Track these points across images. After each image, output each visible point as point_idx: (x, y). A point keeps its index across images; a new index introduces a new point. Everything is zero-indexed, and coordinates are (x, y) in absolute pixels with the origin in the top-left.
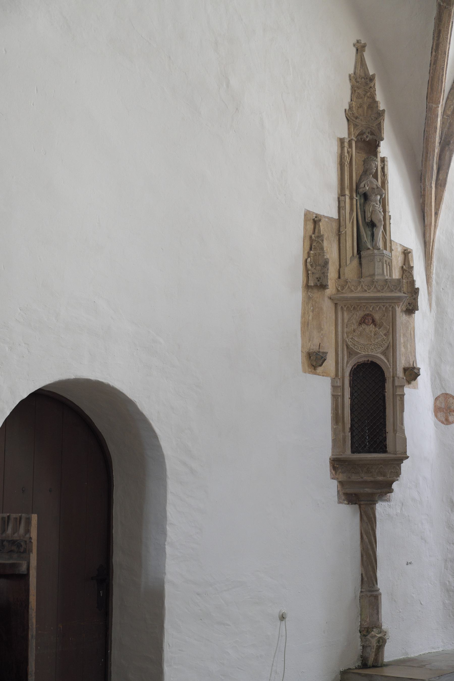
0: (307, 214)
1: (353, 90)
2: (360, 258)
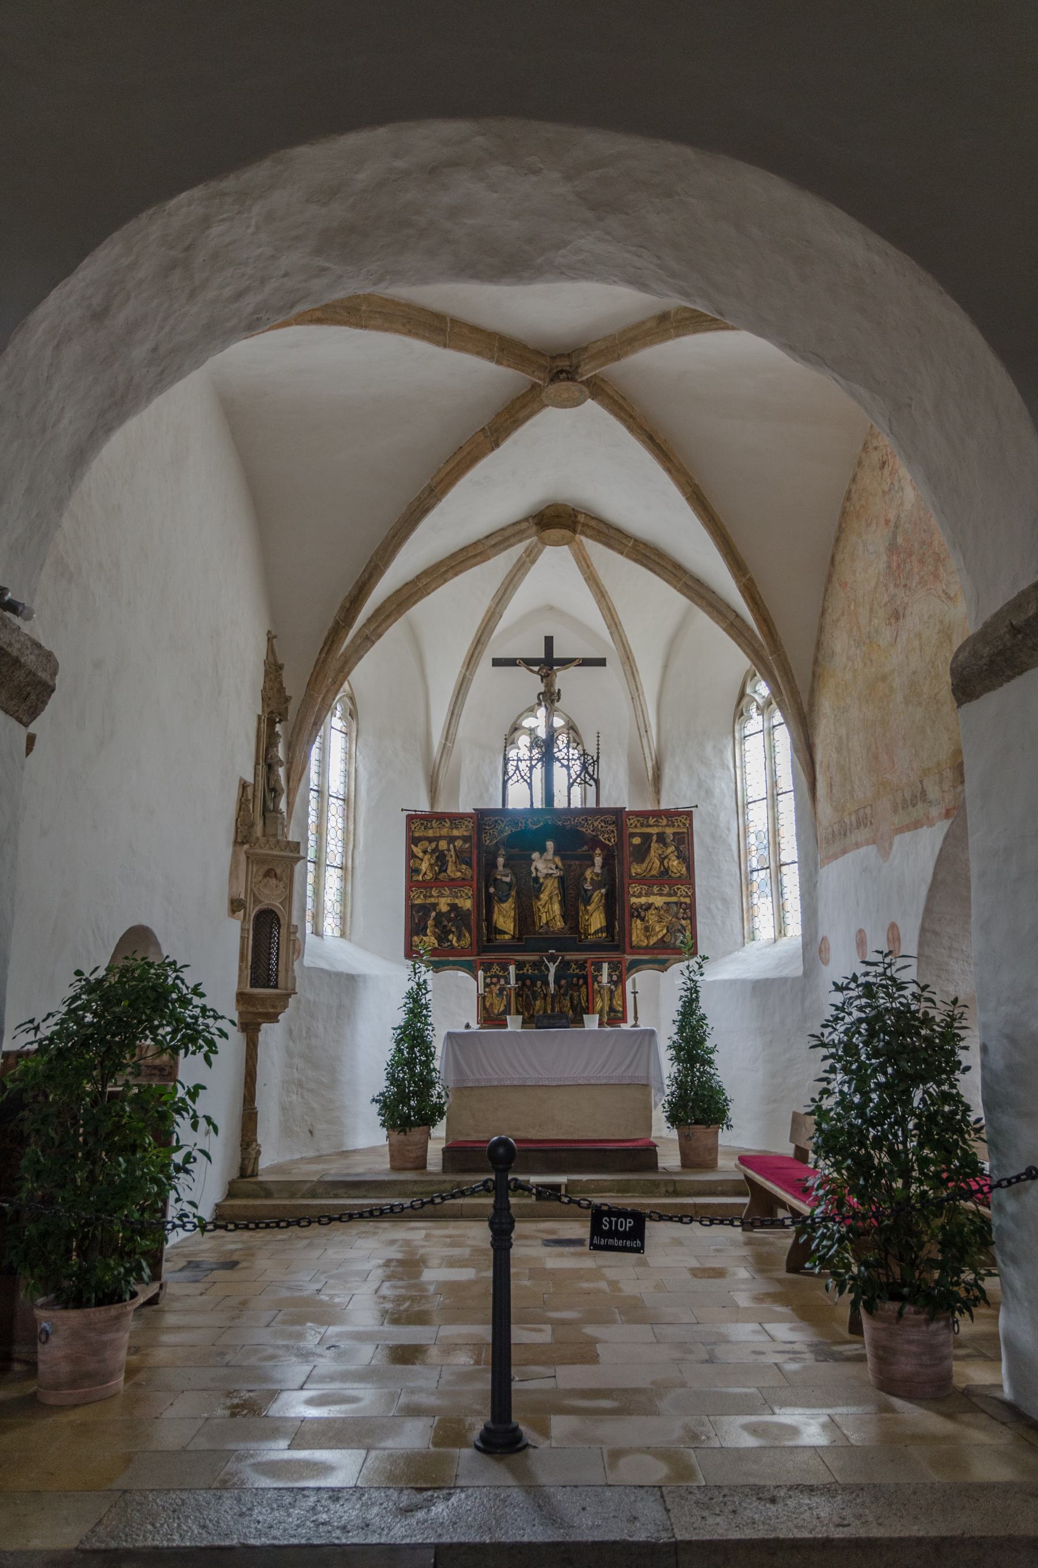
0: (241, 779)
1: (267, 673)
2: (264, 818)
